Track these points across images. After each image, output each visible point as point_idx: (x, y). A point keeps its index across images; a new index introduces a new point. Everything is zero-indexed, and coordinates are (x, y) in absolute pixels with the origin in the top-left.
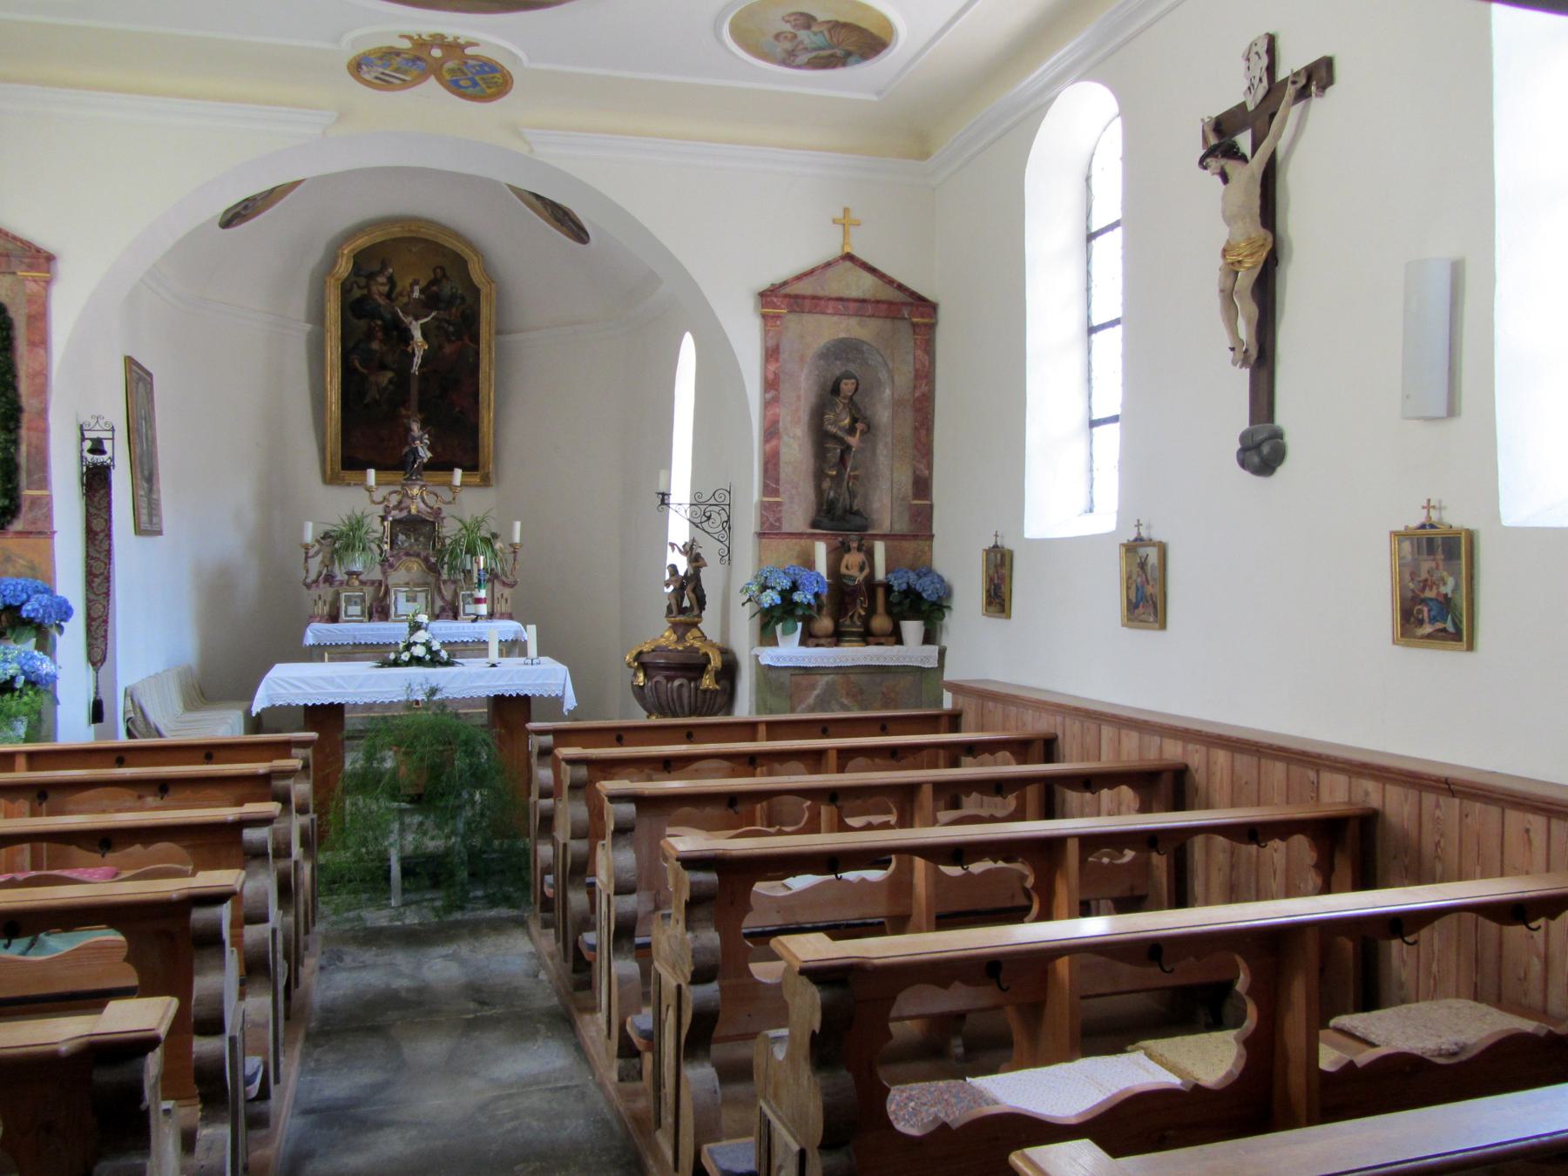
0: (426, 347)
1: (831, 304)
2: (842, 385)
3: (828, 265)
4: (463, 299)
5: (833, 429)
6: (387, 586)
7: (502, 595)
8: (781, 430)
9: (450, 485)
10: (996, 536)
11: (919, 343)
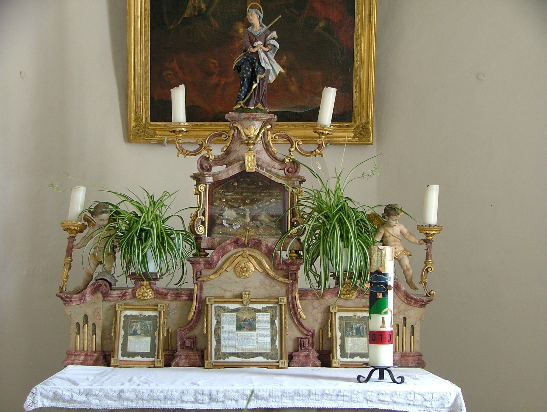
6: (202, 302)
7: (405, 319)
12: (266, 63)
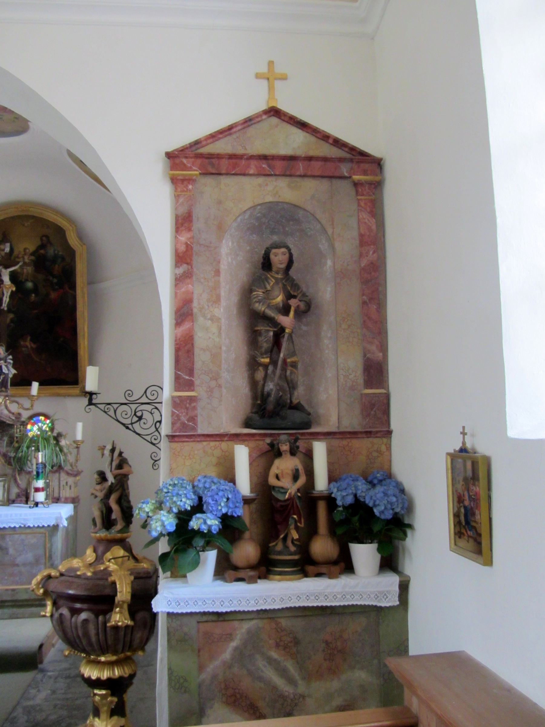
0: (14, 289)
1: (253, 163)
2: (272, 256)
3: (248, 122)
4: (63, 259)
5: (260, 307)
7: (67, 483)
8: (195, 310)
9: (30, 397)
10: (464, 434)
11: (362, 204)
12: (5, 370)
